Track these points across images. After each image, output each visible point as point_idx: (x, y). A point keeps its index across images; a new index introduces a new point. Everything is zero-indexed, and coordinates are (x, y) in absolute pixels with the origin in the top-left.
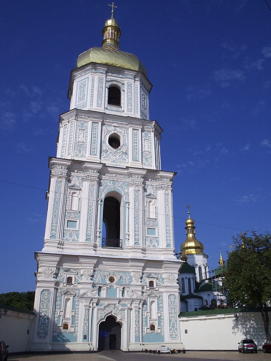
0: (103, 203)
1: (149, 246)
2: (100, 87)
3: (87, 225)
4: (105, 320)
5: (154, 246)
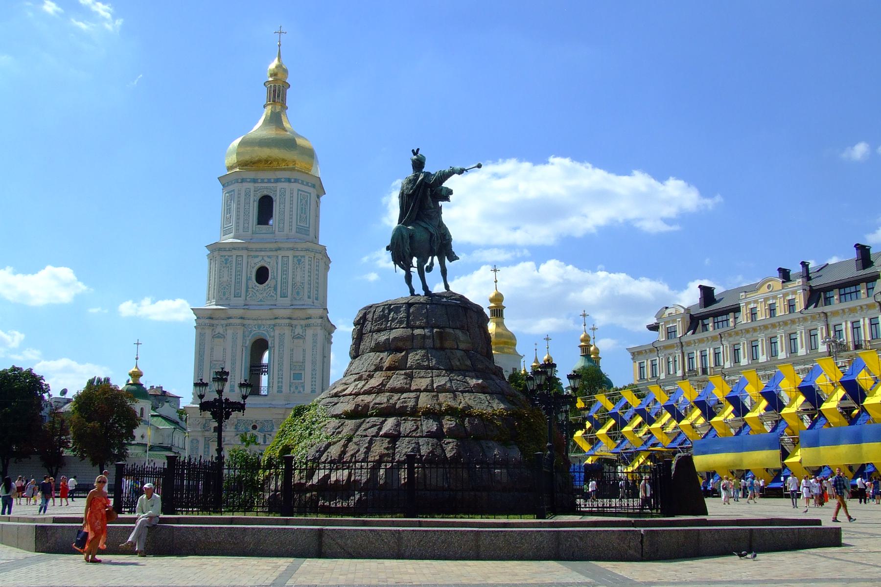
0: (249, 348)
1: (294, 392)
5: (300, 392)
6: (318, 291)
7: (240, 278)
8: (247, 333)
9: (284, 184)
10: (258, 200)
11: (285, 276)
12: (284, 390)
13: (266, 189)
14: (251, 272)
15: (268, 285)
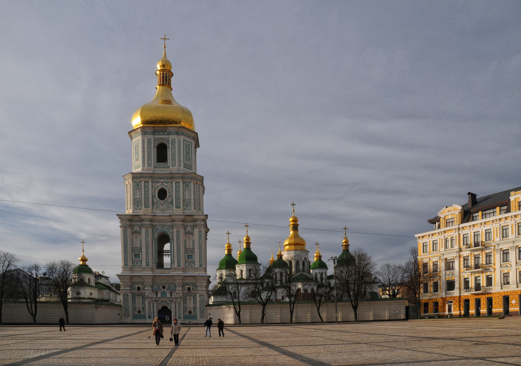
2: (149, 148)
4: (160, 309)
7: (147, 196)
8: (155, 231)
9: (174, 136)
10: (156, 147)
11: (178, 195)
13: (161, 137)
14: (155, 192)
15: (167, 200)
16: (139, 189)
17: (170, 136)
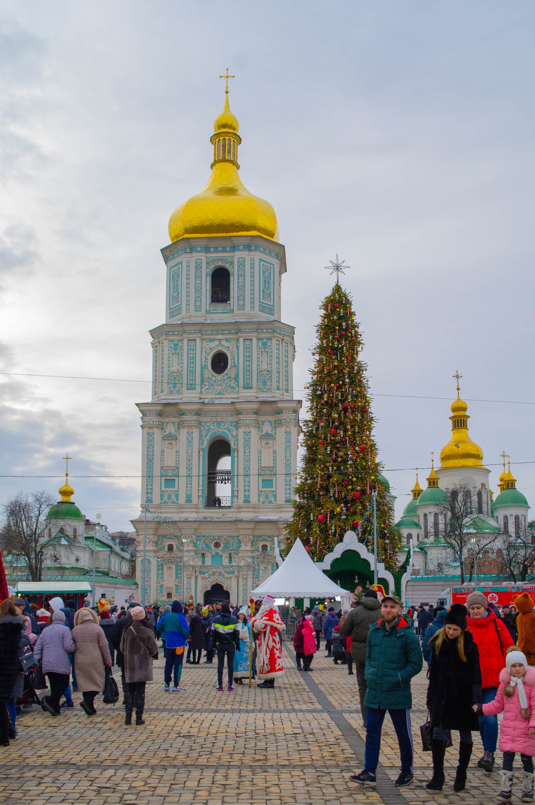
1: (263, 502)
3: (187, 484)
4: (209, 589)
5: (270, 502)
6: (287, 381)
7: (193, 367)
8: (204, 433)
10: (210, 274)
12: (251, 500)
15: (227, 374)
16: (178, 353)
17: (236, 253)
